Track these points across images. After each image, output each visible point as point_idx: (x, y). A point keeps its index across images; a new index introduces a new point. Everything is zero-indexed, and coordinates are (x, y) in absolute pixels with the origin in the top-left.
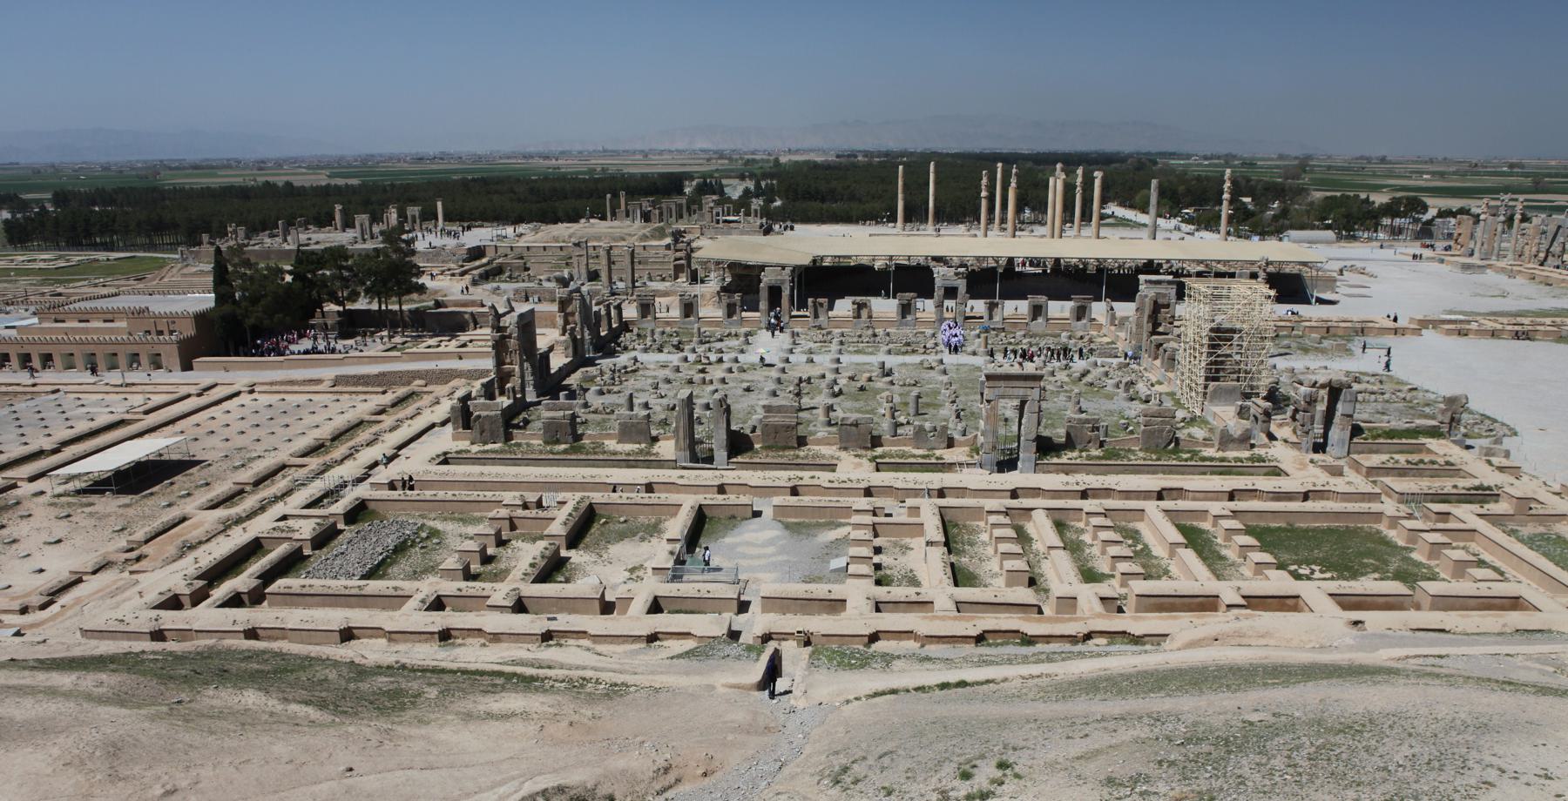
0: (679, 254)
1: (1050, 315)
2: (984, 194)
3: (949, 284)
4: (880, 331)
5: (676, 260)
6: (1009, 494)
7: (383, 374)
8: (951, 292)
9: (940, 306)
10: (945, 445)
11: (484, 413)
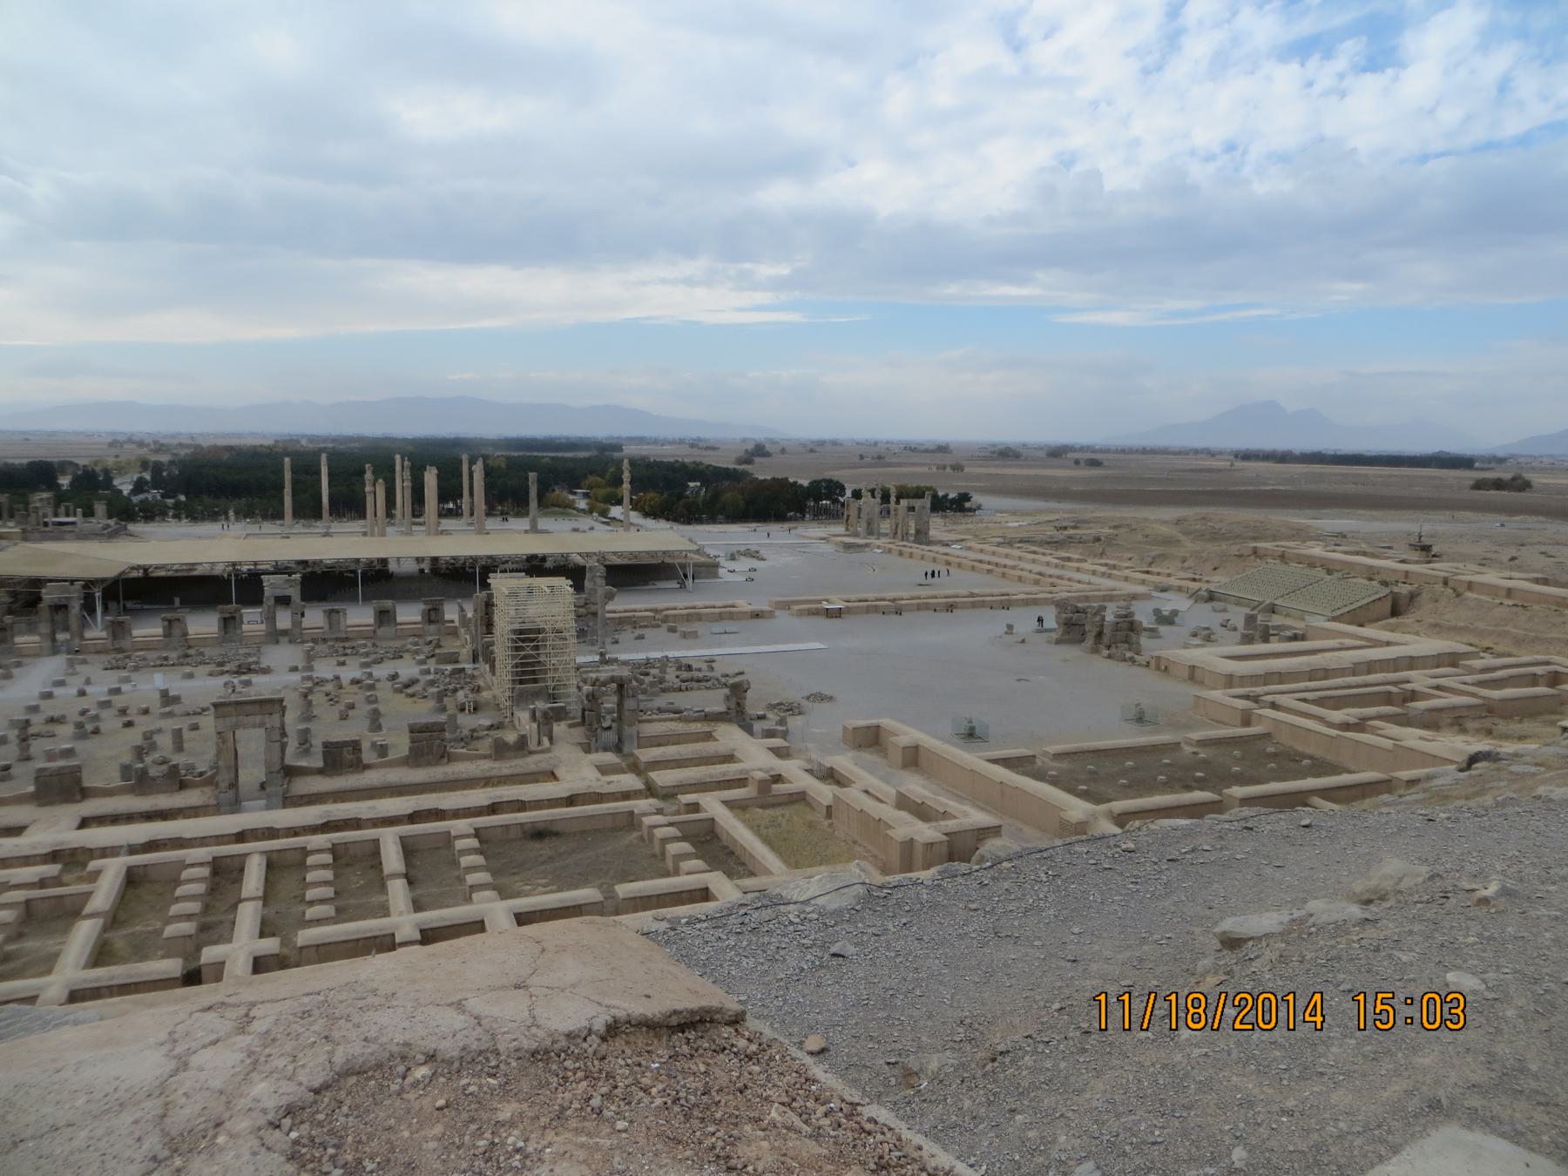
1: (399, 619)
2: (368, 488)
3: (279, 593)
4: (191, 652)
6: (234, 837)
8: (283, 601)
9: (271, 619)
10: (177, 787)
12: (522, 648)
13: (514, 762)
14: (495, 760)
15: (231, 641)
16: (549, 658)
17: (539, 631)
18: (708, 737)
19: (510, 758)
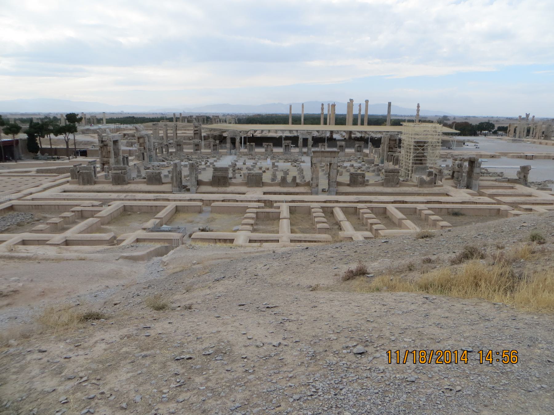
0: (196, 129)
5: (195, 131)
7: (57, 169)
10: (296, 185)
11: (84, 171)
12: (418, 149)
13: (428, 189)
14: (420, 187)
15: (287, 154)
16: (429, 153)
17: (425, 142)
18: (512, 188)
19: (426, 187)
